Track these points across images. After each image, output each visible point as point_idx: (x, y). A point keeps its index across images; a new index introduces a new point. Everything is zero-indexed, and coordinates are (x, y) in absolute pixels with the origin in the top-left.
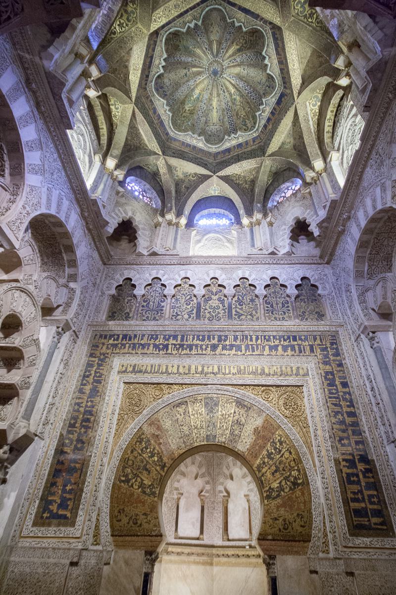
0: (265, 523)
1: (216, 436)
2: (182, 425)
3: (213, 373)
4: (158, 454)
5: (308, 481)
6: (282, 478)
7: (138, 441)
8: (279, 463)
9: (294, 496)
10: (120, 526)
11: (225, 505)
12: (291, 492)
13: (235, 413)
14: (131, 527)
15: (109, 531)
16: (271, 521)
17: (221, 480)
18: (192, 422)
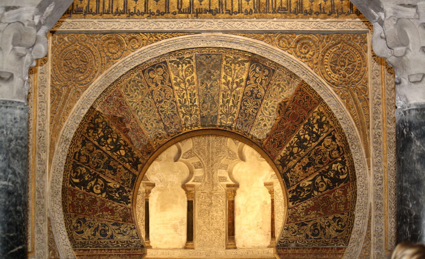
0: (287, 229)
1: (216, 117)
2: (160, 102)
3: (210, 11)
4: (126, 145)
5: (355, 176)
6: (318, 174)
7: (91, 128)
8: (315, 154)
9: (332, 196)
10: (83, 239)
11: (232, 199)
12: (328, 190)
13: (248, 79)
14: (99, 239)
15: (69, 243)
16: (296, 227)
17: (223, 161)
18: (177, 97)
